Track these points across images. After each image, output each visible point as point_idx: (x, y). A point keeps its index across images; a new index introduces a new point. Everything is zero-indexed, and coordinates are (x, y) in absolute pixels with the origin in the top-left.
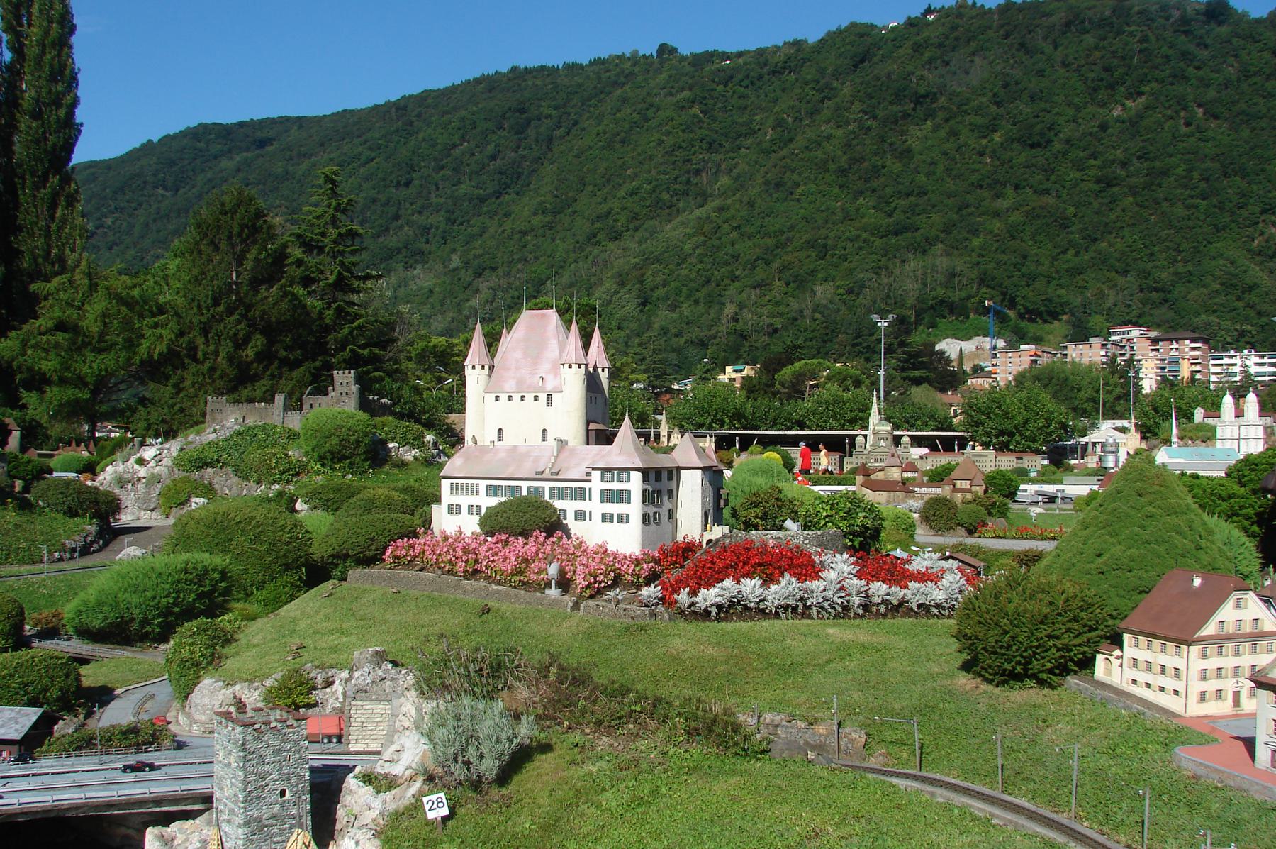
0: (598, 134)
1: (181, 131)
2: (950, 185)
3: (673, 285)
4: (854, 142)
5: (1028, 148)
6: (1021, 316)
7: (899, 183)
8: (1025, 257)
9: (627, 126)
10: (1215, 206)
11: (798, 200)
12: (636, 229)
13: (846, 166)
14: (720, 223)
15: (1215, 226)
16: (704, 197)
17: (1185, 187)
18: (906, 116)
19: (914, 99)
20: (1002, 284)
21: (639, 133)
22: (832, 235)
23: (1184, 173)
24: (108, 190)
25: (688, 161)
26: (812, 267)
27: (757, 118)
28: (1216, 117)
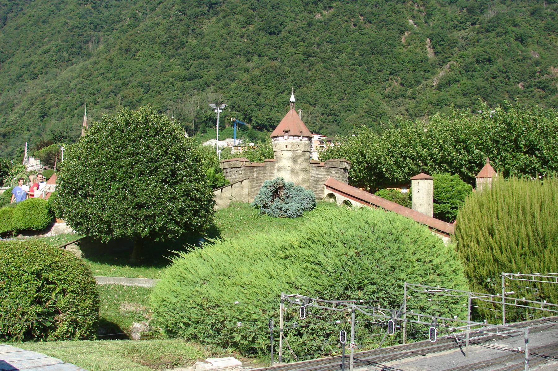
0: (30, 17)
2: (223, 53)
3: (62, 106)
4: (172, 28)
5: (268, 34)
6: (255, 128)
7: (195, 52)
8: (259, 95)
9: (47, 13)
10: (366, 70)
11: (138, 60)
12: (46, 73)
13: (166, 41)
14: (93, 70)
15: (365, 81)
16: (89, 56)
17: (351, 59)
18: (203, 14)
19: (208, 5)
20: (244, 109)
21: (54, 17)
22: (153, 79)
23: (351, 52)
25: (82, 35)
26: (140, 97)
27: (124, 12)
28: (370, 22)
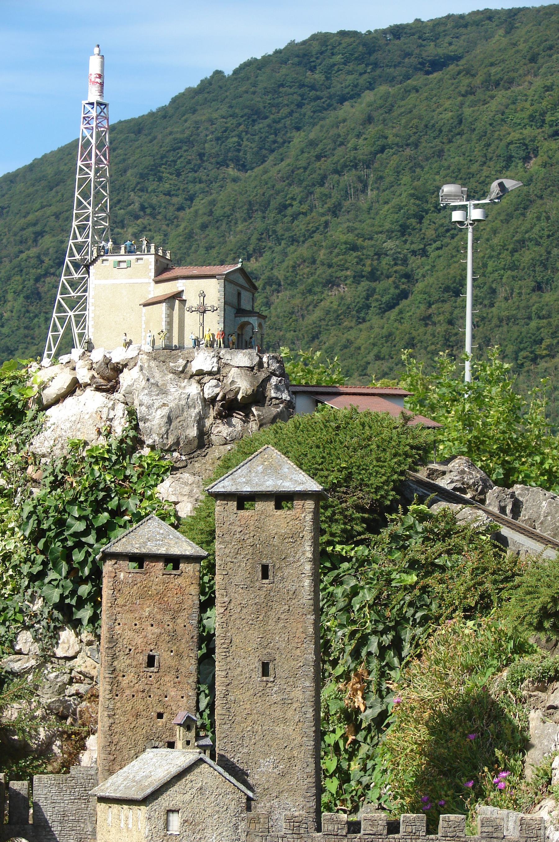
1: (277, 52)
24: (129, 173)
